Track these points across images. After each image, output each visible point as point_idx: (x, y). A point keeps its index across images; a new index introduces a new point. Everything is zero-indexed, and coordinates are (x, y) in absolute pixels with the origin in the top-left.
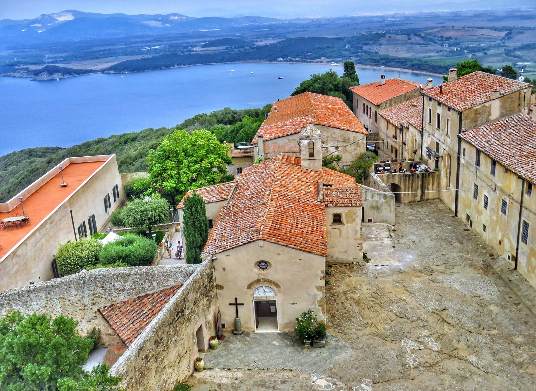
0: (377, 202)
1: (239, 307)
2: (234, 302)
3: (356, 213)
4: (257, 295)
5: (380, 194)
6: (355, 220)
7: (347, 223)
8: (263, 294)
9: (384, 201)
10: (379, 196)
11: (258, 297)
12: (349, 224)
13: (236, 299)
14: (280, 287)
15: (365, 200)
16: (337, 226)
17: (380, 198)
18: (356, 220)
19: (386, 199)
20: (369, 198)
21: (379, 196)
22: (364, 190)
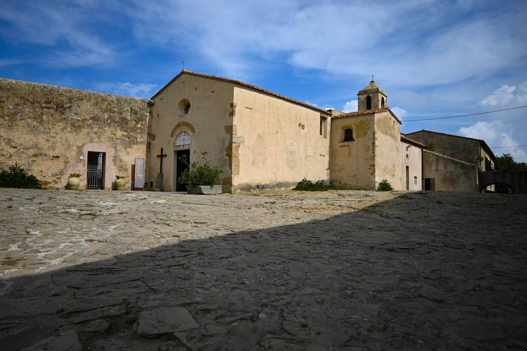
0: (452, 173)
1: (164, 159)
2: (160, 154)
3: (368, 124)
4: (179, 144)
5: (456, 163)
6: (366, 134)
7: (357, 138)
8: (184, 141)
9: (462, 171)
10: (454, 166)
11: (178, 146)
12: (360, 139)
13: (162, 149)
14: (195, 131)
15: (437, 170)
16: (346, 143)
17: (456, 168)
18: (368, 132)
19: (464, 169)
20: (441, 167)
21: (454, 166)
22: (434, 157)
